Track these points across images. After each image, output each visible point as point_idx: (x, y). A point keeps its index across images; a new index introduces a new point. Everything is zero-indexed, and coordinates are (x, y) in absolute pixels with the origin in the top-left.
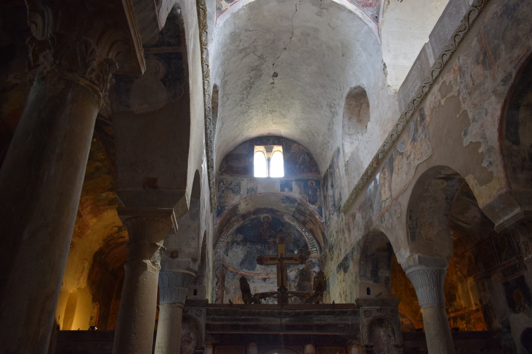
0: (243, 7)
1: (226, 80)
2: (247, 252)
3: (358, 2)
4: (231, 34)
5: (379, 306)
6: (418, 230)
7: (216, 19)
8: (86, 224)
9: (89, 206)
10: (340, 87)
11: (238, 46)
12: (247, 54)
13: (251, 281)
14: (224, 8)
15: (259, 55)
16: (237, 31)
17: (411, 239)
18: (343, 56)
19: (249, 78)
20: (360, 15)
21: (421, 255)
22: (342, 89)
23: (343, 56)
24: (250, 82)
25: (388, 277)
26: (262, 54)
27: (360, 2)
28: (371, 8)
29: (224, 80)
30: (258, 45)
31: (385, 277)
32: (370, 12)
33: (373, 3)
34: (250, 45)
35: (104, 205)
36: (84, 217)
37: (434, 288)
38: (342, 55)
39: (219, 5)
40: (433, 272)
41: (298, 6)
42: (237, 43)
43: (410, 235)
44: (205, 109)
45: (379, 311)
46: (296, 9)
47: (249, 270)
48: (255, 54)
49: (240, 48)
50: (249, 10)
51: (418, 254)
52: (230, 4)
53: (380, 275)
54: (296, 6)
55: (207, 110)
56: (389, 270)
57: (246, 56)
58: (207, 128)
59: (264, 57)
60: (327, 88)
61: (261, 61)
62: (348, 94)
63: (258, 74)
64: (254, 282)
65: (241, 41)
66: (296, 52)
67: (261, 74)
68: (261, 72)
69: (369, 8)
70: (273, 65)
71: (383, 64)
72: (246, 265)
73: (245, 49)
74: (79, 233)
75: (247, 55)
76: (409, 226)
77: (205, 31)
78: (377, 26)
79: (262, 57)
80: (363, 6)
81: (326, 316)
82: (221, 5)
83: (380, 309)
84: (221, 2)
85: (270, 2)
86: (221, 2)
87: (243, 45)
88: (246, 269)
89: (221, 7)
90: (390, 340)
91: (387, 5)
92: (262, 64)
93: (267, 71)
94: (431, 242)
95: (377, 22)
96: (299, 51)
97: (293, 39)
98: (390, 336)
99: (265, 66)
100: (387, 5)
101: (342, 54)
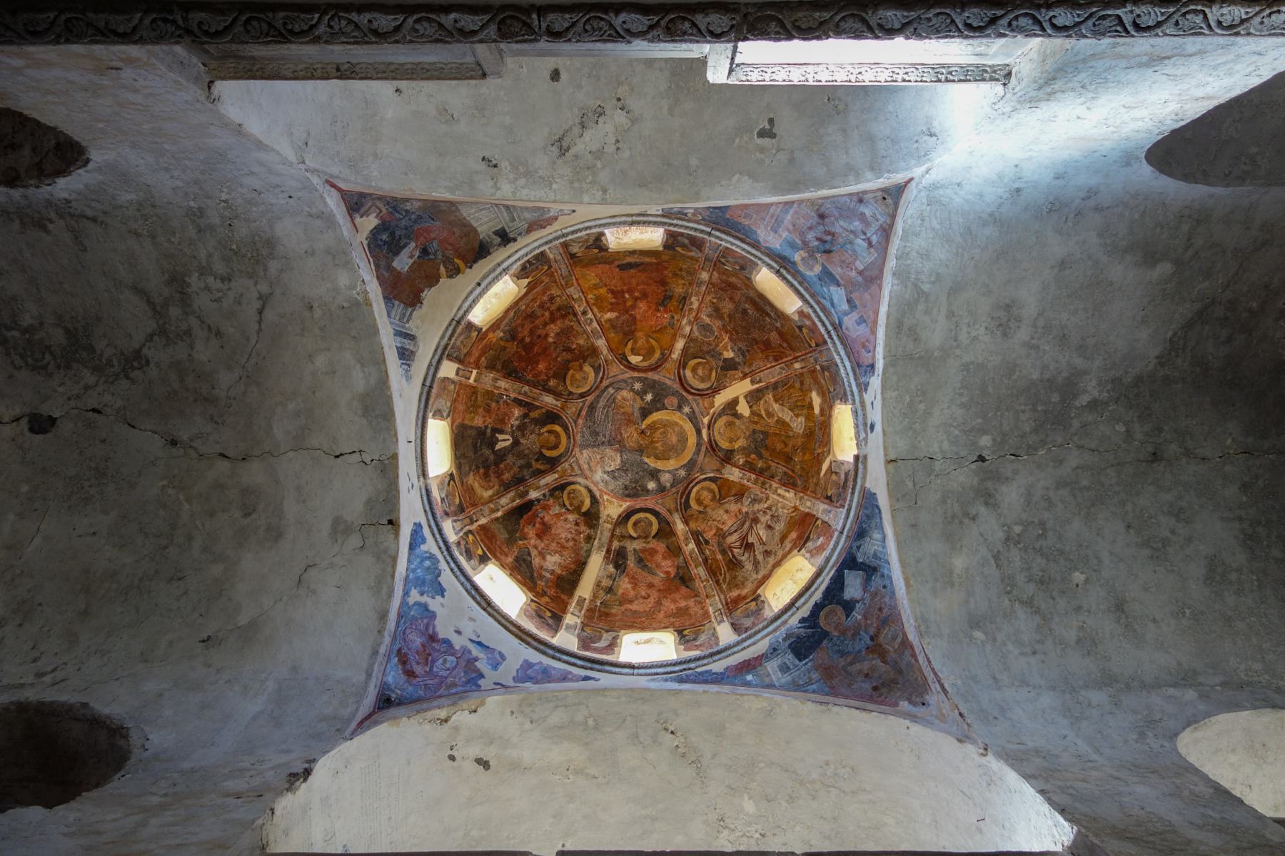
0: (363, 281)
1: (51, 227)
3: (404, 633)
4: (270, 243)
7: (339, 189)
10: (54, 670)
11: (204, 271)
12: (158, 308)
14: (358, 220)
15: (145, 351)
16: (274, 266)
18: (203, 641)
19: (27, 320)
20: (382, 650)
22: (47, 679)
23: (203, 641)
24: (9, 329)
26: (148, 362)
27: (404, 639)
28: (403, 678)
29: (53, 215)
30: (192, 347)
32: (393, 676)
33: (418, 679)
34: (198, 317)
38: (204, 636)
39: (369, 204)
41: (356, 457)
42: (220, 267)
46: (341, 455)
48: (150, 337)
49: (194, 280)
50: (346, 305)
52: (365, 243)
54: (354, 452)
57: (150, 303)
58: (171, 12)
59: (136, 374)
60: (20, 625)
61: (115, 363)
62: (43, 703)
63: (47, 357)
65: (222, 280)
66: (165, 482)
67: (44, 367)
68: (59, 367)
69: (401, 672)
70: (94, 410)
71: (306, 765)
73: (184, 298)
75: (154, 309)
77: (732, 26)
78: (371, 709)
79: (136, 364)
80: (399, 650)
82: (366, 214)
84: (375, 211)
85: (366, 370)
86: (375, 215)
87: (208, 289)
89: (362, 211)
91: (438, 719)
92: (97, 370)
93: (61, 389)
95: (380, 709)
96: (170, 491)
97: (223, 465)
99: (90, 379)
100: (438, 719)
101: (209, 638)
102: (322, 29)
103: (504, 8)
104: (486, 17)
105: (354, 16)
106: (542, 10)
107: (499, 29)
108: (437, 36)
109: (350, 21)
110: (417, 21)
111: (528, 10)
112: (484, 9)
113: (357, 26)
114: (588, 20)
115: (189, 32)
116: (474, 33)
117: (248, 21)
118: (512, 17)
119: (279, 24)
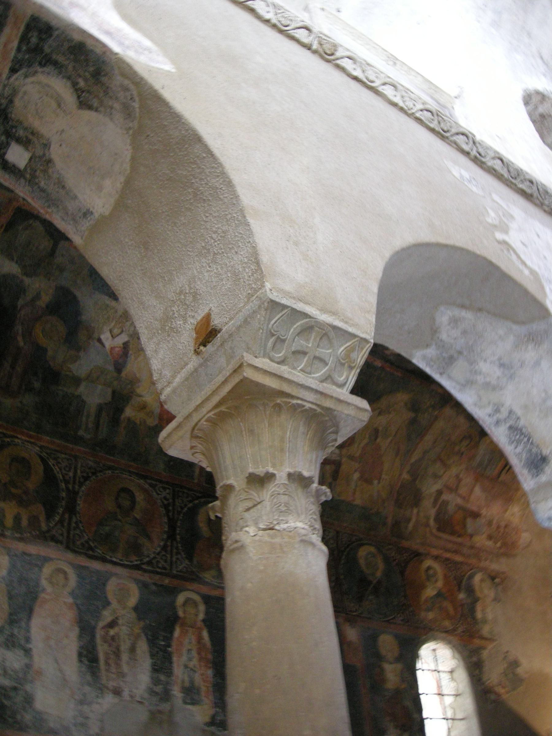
8: (503, 524)
9: (474, 486)
35: (502, 470)
36: (484, 512)
44: (419, 120)
55: (423, 118)
58: (476, 157)
74: (500, 548)
102: (420, 106)
103: (328, 61)
104: (338, 62)
105: (401, 104)
106: (308, 47)
107: (336, 50)
108: (369, 68)
109: (404, 102)
110: (372, 82)
111: (315, 52)
112: (338, 67)
113: (403, 97)
114: (286, 26)
115: (474, 143)
116: (349, 58)
117: (448, 131)
118: (326, 53)
119: (436, 122)
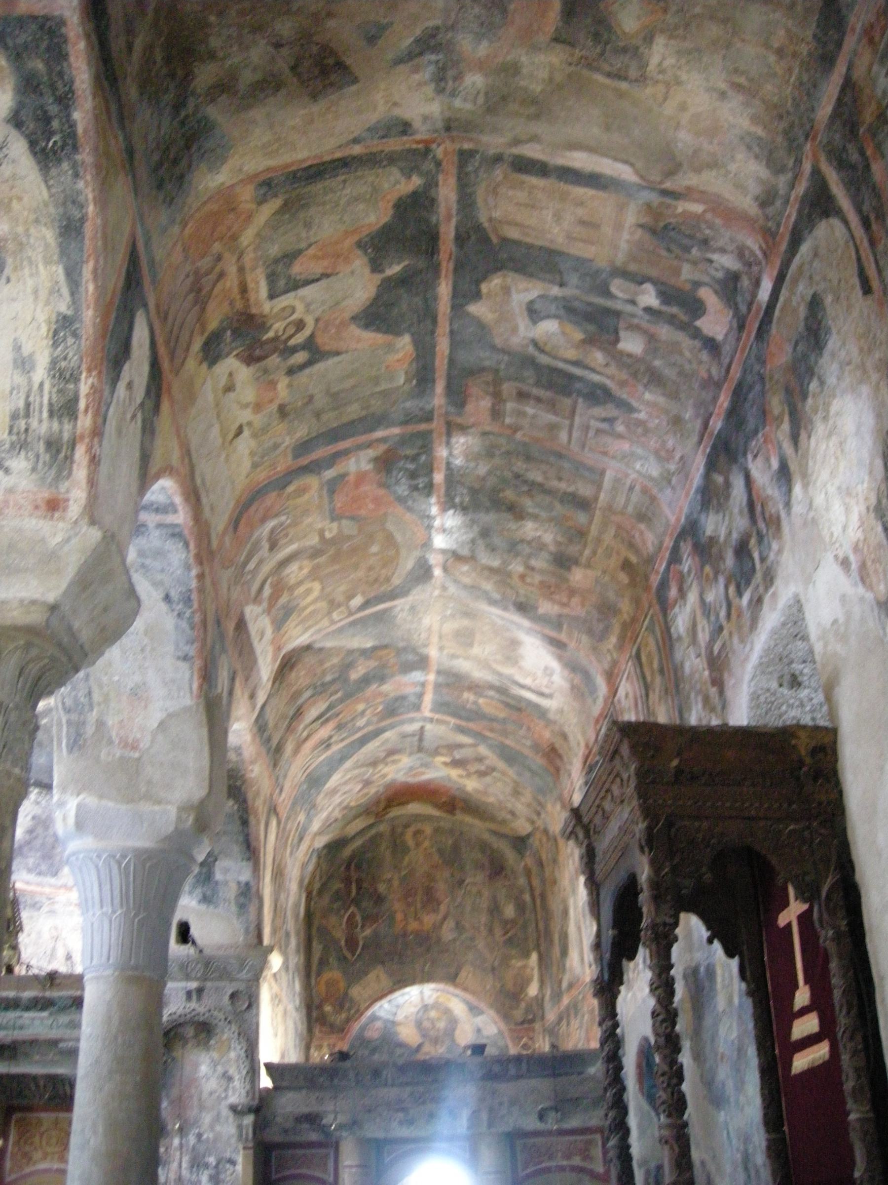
2: (34, 818)
5: (197, 979)
6: (95, 712)
13: (45, 909)
17: (67, 747)
21: (91, 800)
25: (247, 884)
31: (239, 883)
37: (114, 912)
40: (114, 857)
43: (68, 732)
45: (194, 997)
47: (40, 874)
51: (81, 797)
53: (218, 876)
56: (249, 859)
64: (52, 912)
72: (31, 861)
76: (63, 703)
81: (27, 1015)
83: (200, 991)
88: (30, 871)
90: (226, 1090)
94: (136, 755)
98: (230, 1079)
